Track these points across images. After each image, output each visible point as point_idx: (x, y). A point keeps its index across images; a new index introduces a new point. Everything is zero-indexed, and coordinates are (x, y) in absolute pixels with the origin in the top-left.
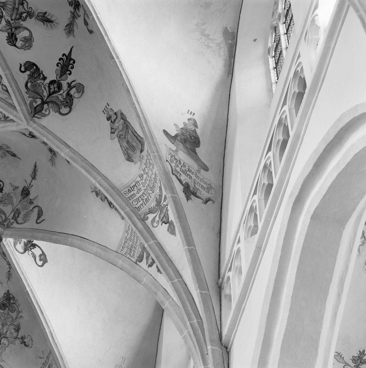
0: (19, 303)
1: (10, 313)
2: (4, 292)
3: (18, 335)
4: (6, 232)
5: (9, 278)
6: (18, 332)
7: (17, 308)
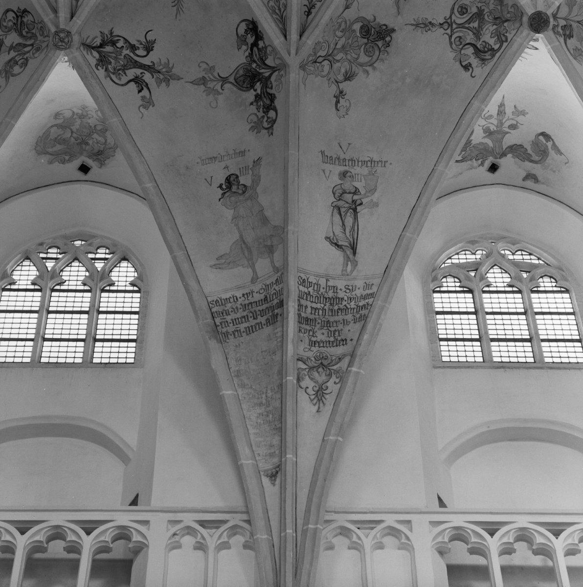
0: (386, 59)
1: (362, 49)
2: (387, 23)
3: (342, 82)
4: (550, 33)
5: (417, 25)
6: (345, 81)
7: (375, 58)
